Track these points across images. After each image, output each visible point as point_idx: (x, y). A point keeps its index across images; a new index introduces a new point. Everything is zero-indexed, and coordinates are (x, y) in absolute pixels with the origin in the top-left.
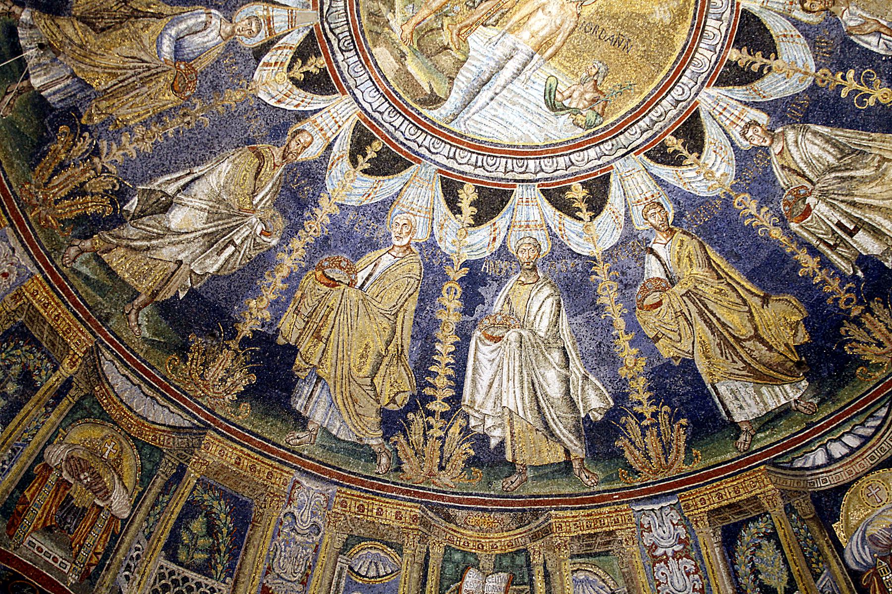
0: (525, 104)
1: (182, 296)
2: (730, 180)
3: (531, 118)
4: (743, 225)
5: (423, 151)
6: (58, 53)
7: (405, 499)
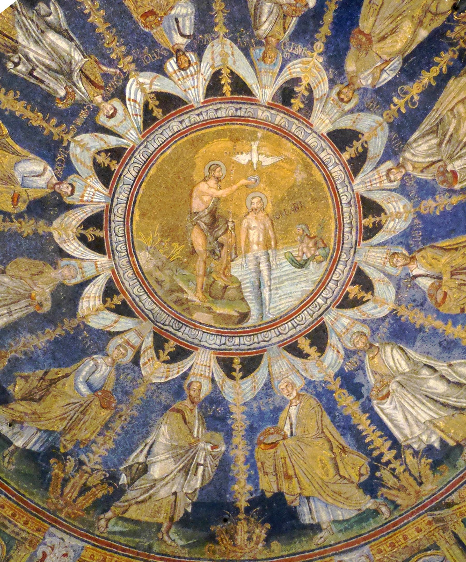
0: (287, 277)
1: (189, 510)
2: (409, 205)
4: (438, 216)
5: (263, 344)
6: (22, 423)
7: (414, 519)
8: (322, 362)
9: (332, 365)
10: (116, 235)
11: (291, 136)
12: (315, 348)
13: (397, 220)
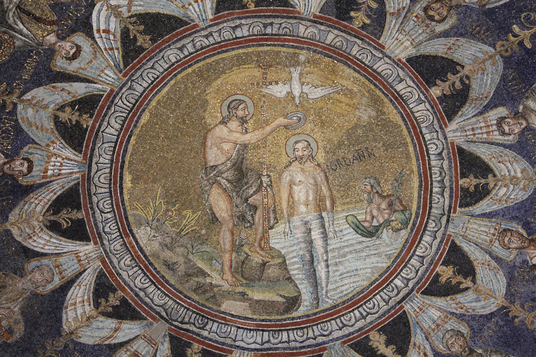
0: (351, 249)
3: (365, 254)
5: (320, 339)
11: (352, 61)
13: (512, 187)
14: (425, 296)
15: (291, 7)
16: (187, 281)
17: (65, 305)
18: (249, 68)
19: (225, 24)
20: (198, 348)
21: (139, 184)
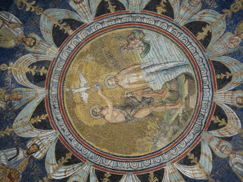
3: (159, 47)
5: (205, 62)
8: (212, 23)
9: (214, 16)
10: (150, 164)
12: (203, 29)
14: (174, 17)
15: (44, 99)
16: (182, 124)
17: (194, 178)
18: (76, 111)
19: (57, 124)
20: (214, 118)
21: (136, 149)
